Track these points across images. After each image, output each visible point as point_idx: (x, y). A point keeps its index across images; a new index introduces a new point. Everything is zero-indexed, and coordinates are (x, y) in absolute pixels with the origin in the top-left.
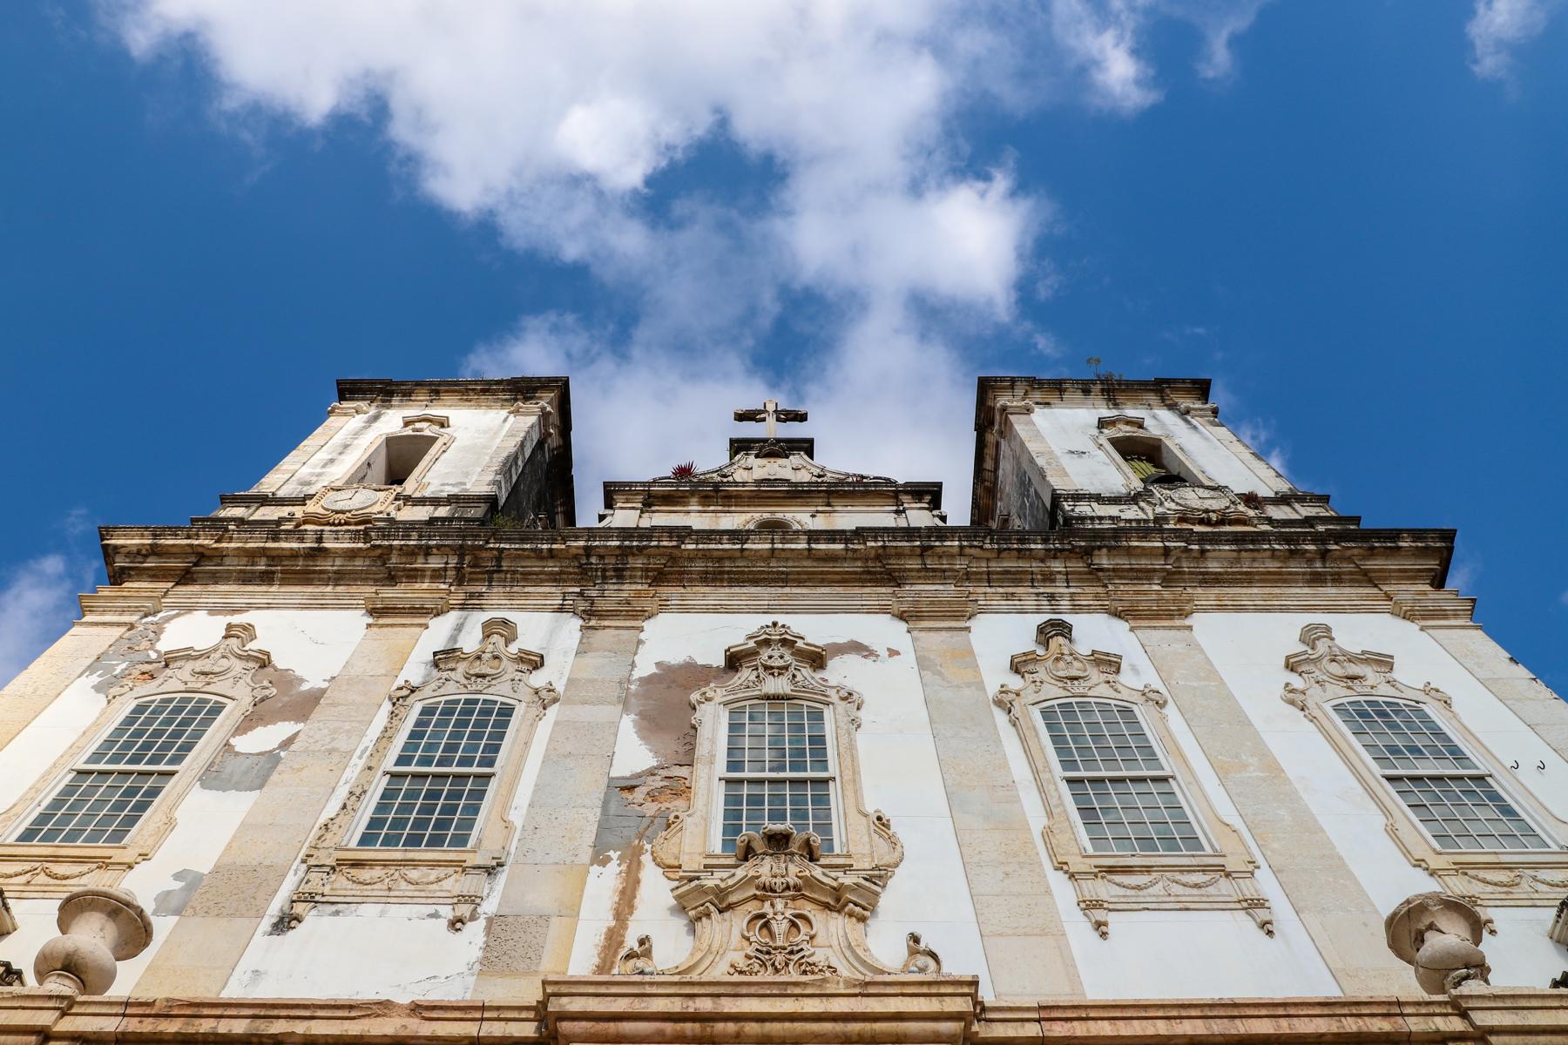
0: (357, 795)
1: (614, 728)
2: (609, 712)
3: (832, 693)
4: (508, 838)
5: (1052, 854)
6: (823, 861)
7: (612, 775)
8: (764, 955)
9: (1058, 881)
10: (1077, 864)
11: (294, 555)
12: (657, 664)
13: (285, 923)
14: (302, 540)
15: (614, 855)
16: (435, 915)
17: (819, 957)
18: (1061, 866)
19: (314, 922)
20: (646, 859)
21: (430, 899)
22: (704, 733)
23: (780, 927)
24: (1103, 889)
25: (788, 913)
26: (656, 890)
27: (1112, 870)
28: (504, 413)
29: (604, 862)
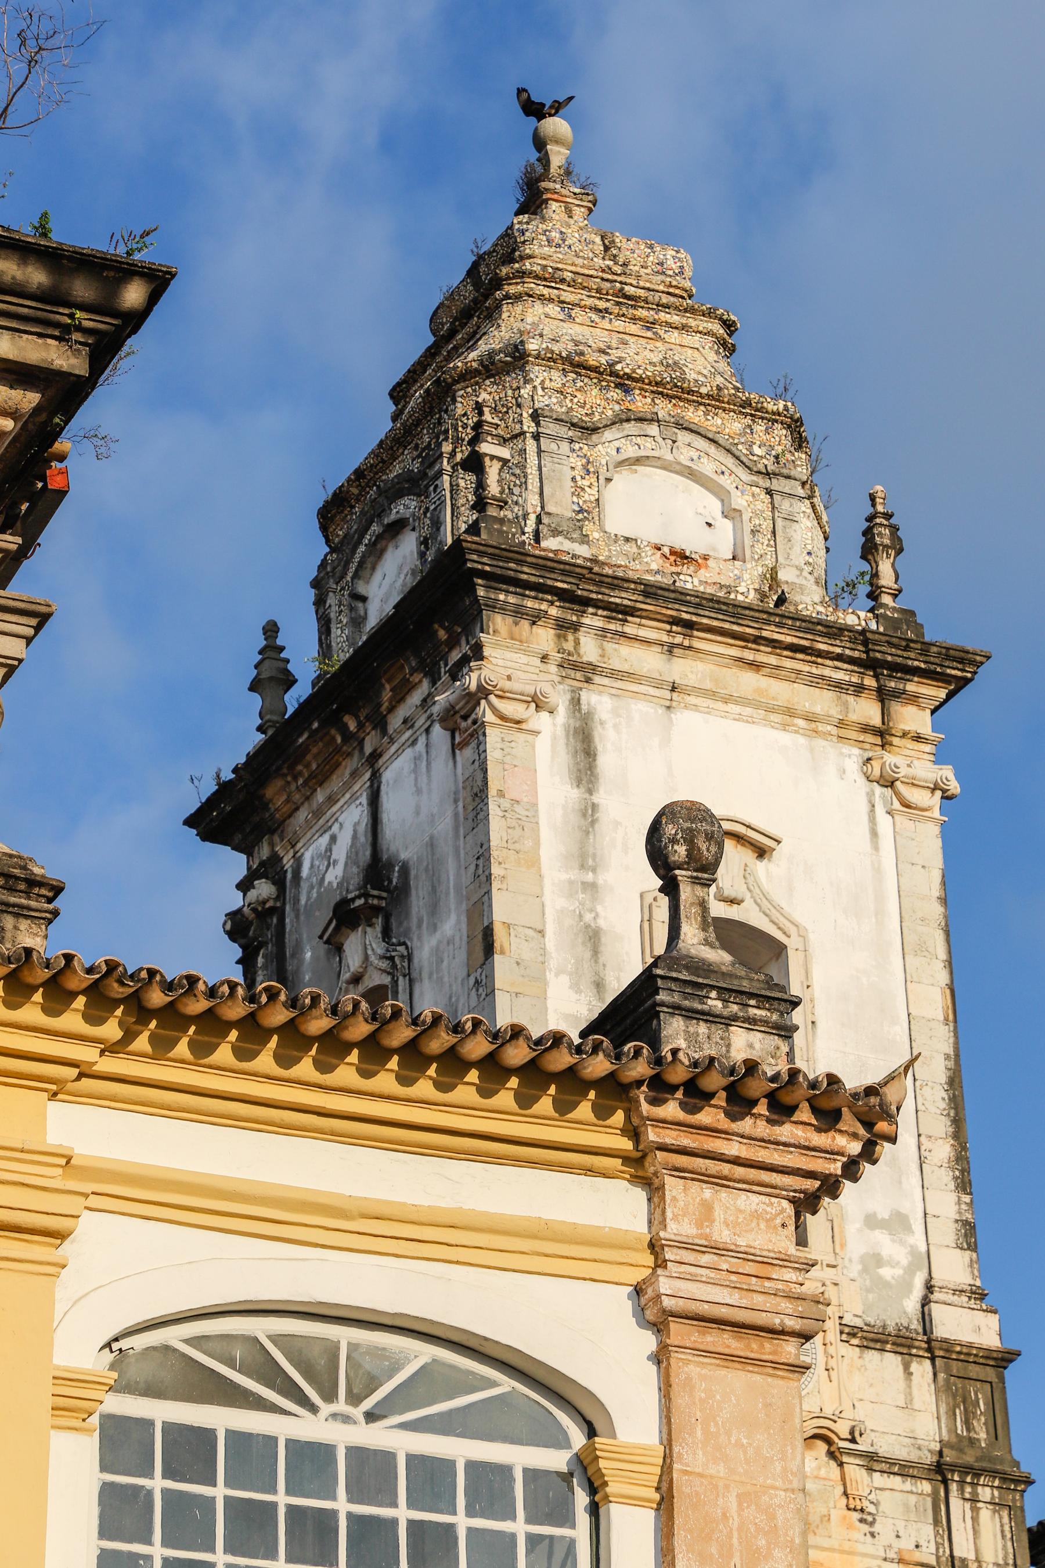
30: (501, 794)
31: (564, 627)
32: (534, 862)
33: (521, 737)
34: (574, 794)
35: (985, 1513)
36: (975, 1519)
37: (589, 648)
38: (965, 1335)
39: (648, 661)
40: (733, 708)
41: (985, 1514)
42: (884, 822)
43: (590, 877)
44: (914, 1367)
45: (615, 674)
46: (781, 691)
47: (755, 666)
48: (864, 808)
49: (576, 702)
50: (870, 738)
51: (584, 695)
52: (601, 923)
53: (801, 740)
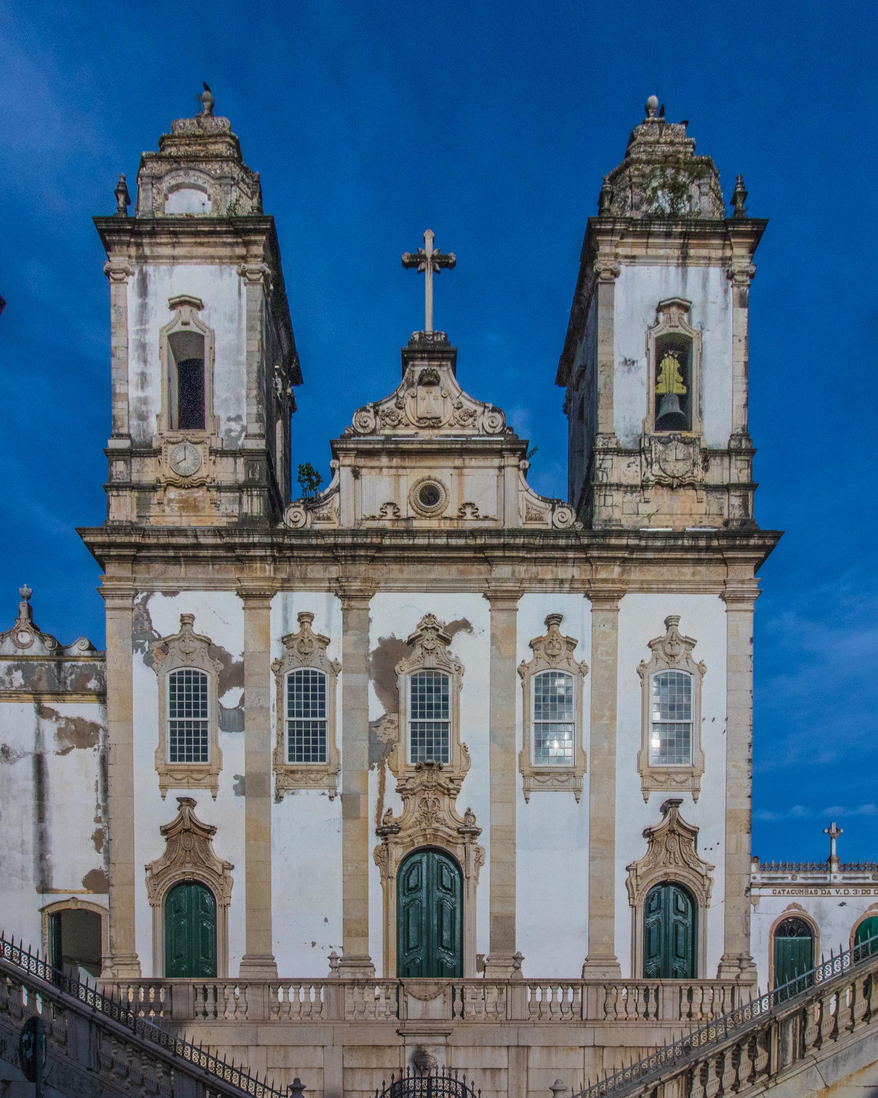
0: (280, 735)
1: (366, 688)
2: (363, 677)
3: (452, 666)
4: (339, 758)
5: (520, 766)
6: (444, 769)
7: (370, 720)
8: (425, 814)
9: (519, 776)
10: (527, 773)
11: (185, 547)
12: (380, 639)
13: (279, 799)
14: (186, 536)
15: (376, 764)
16: (324, 794)
17: (441, 815)
18: (521, 771)
19: (287, 798)
20: (386, 766)
21: (320, 787)
22: (402, 694)
23: (430, 803)
24: (532, 782)
25: (433, 797)
26: (392, 782)
27: (537, 774)
28: (235, 269)
29: (372, 768)
30: (115, 305)
31: (139, 245)
32: (125, 326)
33: (122, 285)
34: (139, 301)
35: (255, 499)
36: (252, 501)
37: (147, 251)
38: (256, 448)
39: (167, 251)
40: (194, 261)
41: (255, 499)
42: (244, 289)
43: (143, 327)
44: (238, 461)
45: (155, 258)
46: (211, 251)
47: (202, 244)
48: (237, 285)
49: (141, 270)
50: (241, 261)
51: (144, 268)
52: (147, 341)
53: (217, 267)
